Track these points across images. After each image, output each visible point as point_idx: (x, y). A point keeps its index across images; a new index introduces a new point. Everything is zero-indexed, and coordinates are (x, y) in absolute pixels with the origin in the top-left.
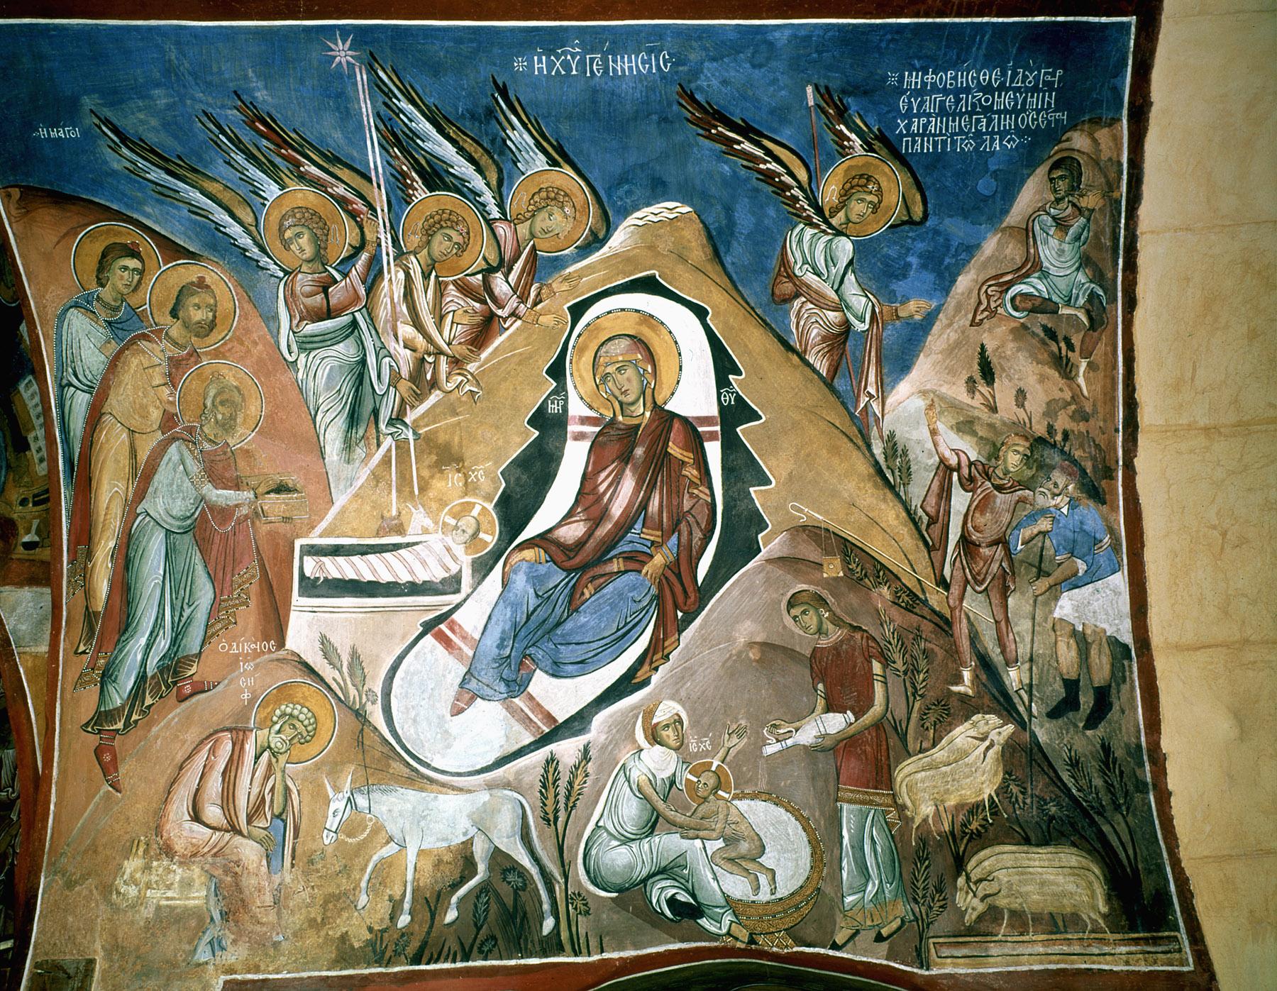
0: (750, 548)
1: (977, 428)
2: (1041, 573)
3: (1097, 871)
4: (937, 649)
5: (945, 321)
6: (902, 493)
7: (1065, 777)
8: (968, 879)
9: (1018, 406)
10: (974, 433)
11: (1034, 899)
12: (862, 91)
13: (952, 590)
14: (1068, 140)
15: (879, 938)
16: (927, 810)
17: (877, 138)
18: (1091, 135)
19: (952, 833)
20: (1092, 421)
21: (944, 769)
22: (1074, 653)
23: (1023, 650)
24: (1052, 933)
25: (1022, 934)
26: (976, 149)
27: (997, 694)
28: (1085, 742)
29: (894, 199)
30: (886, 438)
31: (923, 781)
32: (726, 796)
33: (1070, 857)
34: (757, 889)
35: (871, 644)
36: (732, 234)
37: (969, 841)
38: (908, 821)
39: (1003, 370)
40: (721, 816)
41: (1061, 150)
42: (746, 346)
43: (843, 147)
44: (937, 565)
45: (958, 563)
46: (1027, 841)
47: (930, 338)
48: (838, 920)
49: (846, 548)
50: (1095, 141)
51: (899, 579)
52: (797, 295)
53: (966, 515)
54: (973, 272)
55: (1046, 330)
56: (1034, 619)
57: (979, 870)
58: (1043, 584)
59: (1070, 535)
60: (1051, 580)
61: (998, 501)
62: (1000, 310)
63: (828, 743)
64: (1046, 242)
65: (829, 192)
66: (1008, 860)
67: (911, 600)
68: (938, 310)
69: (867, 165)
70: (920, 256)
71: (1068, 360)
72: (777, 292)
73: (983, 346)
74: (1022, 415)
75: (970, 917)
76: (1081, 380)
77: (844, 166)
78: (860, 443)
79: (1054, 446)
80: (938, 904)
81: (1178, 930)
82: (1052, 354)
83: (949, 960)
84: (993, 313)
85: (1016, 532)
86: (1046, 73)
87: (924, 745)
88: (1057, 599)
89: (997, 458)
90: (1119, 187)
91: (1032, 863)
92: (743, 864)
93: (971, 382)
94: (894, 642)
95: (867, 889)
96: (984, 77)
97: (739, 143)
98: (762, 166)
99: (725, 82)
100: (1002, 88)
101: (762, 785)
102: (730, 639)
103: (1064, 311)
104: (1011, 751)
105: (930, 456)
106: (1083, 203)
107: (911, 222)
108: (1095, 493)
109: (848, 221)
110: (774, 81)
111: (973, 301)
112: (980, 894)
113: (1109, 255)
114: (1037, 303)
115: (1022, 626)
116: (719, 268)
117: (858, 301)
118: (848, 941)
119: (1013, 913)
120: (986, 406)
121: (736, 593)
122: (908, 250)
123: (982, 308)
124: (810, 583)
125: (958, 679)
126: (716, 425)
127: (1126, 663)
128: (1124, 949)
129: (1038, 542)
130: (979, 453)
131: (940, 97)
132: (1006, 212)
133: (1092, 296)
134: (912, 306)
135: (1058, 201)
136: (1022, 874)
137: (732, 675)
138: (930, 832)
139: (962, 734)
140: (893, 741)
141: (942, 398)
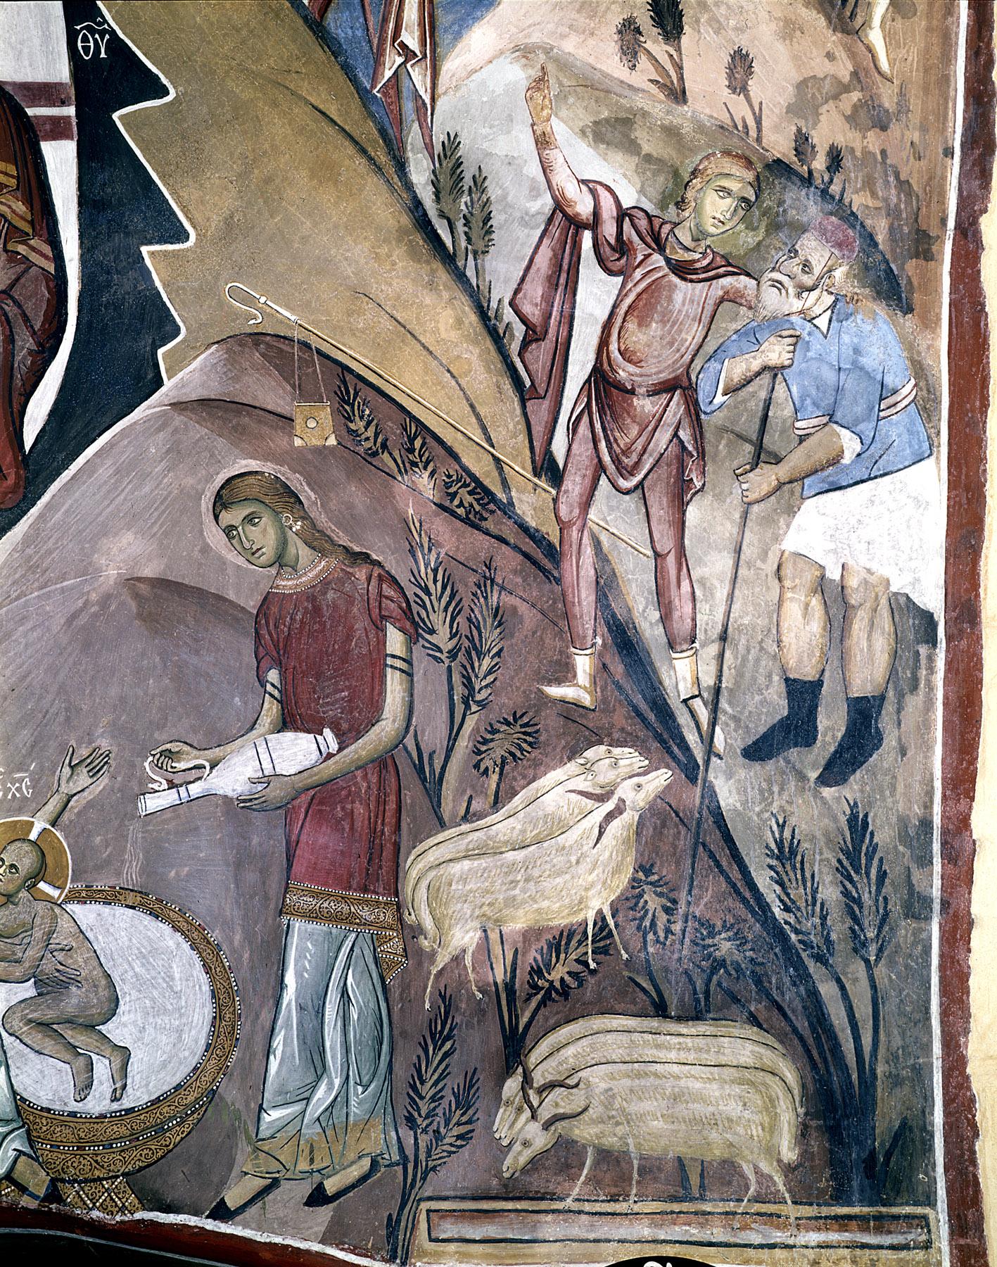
0: (139, 378)
1: (640, 134)
2: (762, 455)
3: (791, 1076)
4: (523, 608)
6: (470, 273)
7: (763, 880)
8: (527, 1080)
9: (732, 88)
10: (631, 147)
11: (653, 1128)
13: (568, 484)
15: (318, 1198)
16: (464, 937)
19: (510, 988)
20: (895, 129)
21: (510, 856)
22: (816, 626)
23: (710, 617)
24: (674, 1199)
25: (613, 1199)
27: (643, 707)
28: (814, 813)
30: (438, 149)
31: (464, 879)
32: (55, 893)
33: (741, 1046)
34: (85, 1087)
35: (388, 590)
37: (542, 1003)
38: (416, 955)
40: (38, 934)
44: (538, 430)
45: (583, 428)
46: (660, 1010)
48: (239, 1158)
49: (347, 388)
51: (455, 456)
53: (607, 326)
56: (739, 551)
57: (552, 1063)
58: (765, 478)
59: (830, 376)
60: (783, 471)
61: (678, 297)
63: (276, 793)
66: (615, 1046)
67: (476, 503)
74: (741, 110)
75: (517, 1159)
76: (875, 37)
78: (383, 158)
79: (808, 180)
80: (456, 1131)
81: (931, 1203)
83: (452, 1247)
85: (714, 365)
87: (475, 806)
88: (791, 511)
89: (681, 204)
91: (662, 1055)
92: (68, 1034)
93: (629, 29)
94: (435, 589)
95: (317, 1094)
101: (131, 875)
102: (88, 570)
104: (659, 822)
105: (534, 193)
108: (891, 290)
112: (545, 1113)
115: (712, 566)
118: (252, 1201)
119: (606, 1156)
120: (662, 87)
121: (104, 471)
124: (266, 457)
125: (564, 672)
126: (63, 103)
127: (923, 650)
128: (814, 1237)
129: (759, 389)
130: (642, 191)
136: (639, 1076)
137: (87, 646)
138: (463, 983)
139: (557, 788)
140: (412, 794)
141: (564, 65)
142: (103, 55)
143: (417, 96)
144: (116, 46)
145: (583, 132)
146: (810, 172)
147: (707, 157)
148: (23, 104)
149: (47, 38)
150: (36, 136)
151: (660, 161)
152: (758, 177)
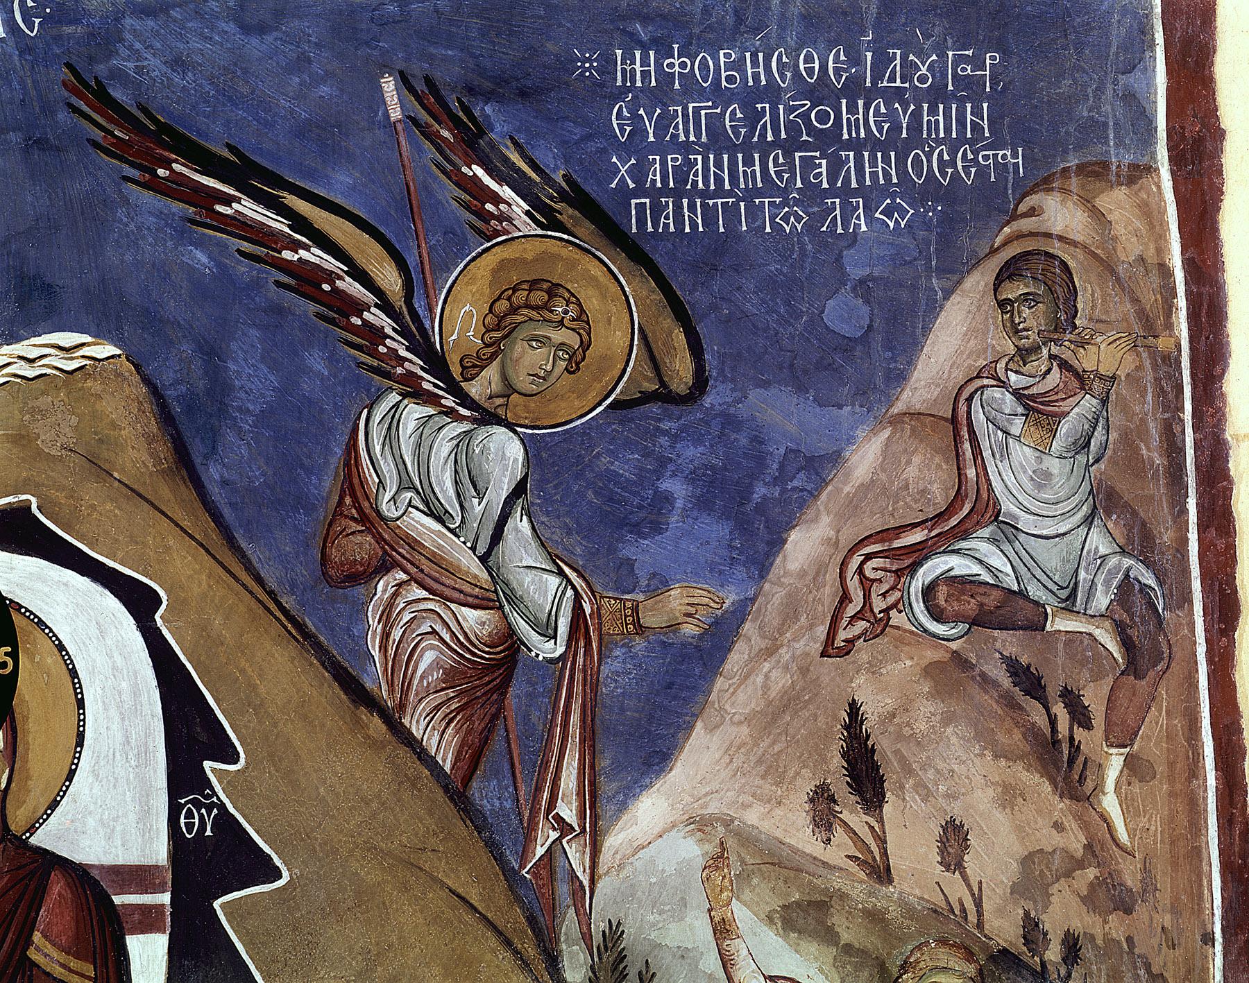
1: (838, 920)
5: (758, 642)
10: (828, 936)
12: (520, 89)
14: (1032, 212)
17: (563, 196)
18: (1087, 203)
20: (1141, 911)
26: (811, 228)
29: (619, 339)
30: (597, 939)
36: (222, 412)
39: (908, 770)
41: (1019, 236)
42: (253, 687)
43: (485, 217)
47: (720, 683)
50: (1097, 215)
52: (385, 567)
54: (825, 520)
55: (1015, 669)
62: (897, 618)
64: (1005, 453)
65: (460, 320)
68: (740, 614)
69: (545, 259)
70: (692, 478)
71: (1075, 748)
72: (334, 555)
73: (854, 708)
74: (957, 891)
76: (1110, 803)
77: (490, 260)
78: (531, 951)
82: (1032, 732)
84: (881, 625)
86: (958, 60)
90: (1169, 326)
93: (822, 799)
96: (809, 63)
97: (228, 200)
98: (287, 255)
99: (178, 63)
100: (853, 89)
103: (1061, 624)
106: (1086, 361)
107: (664, 396)
109: (509, 389)
110: (302, 63)
111: (828, 593)
113: (1160, 489)
114: (992, 600)
116: (189, 494)
117: (542, 588)
120: (862, 863)
122: (663, 462)
123: (851, 610)
126: (160, 889)
131: (706, 108)
132: (899, 377)
133: (1127, 586)
134: (676, 599)
135: (1025, 354)
141: (747, 838)
142: (208, 833)
143: (573, 876)
144: (225, 822)
145: (770, 919)
146: (1043, 964)
147: (919, 947)
148: (109, 891)
149: (145, 813)
150: (121, 929)
151: (862, 952)
152: (980, 972)
